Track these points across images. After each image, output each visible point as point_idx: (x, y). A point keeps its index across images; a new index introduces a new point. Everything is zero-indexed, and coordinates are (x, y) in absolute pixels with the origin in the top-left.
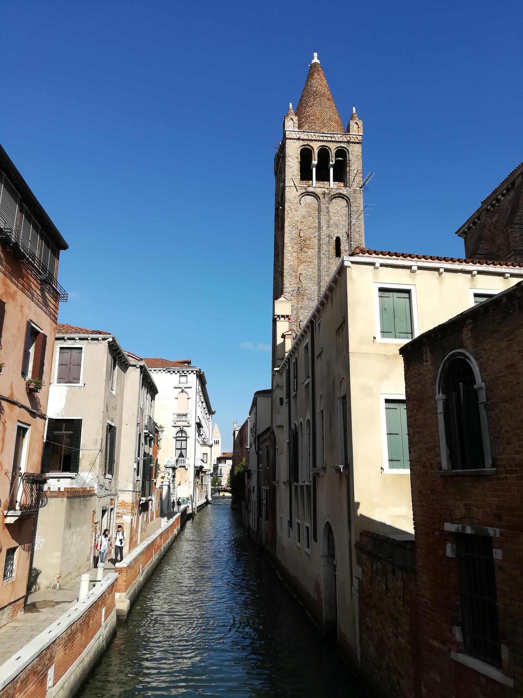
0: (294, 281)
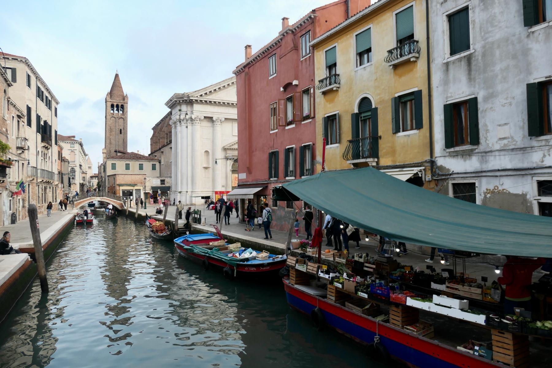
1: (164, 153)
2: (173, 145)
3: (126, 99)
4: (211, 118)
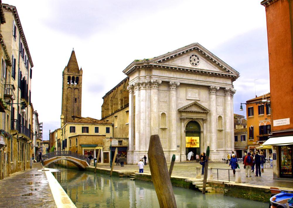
0: (66, 108)
1: (118, 118)
2: (130, 109)
3: (80, 72)
4: (167, 83)
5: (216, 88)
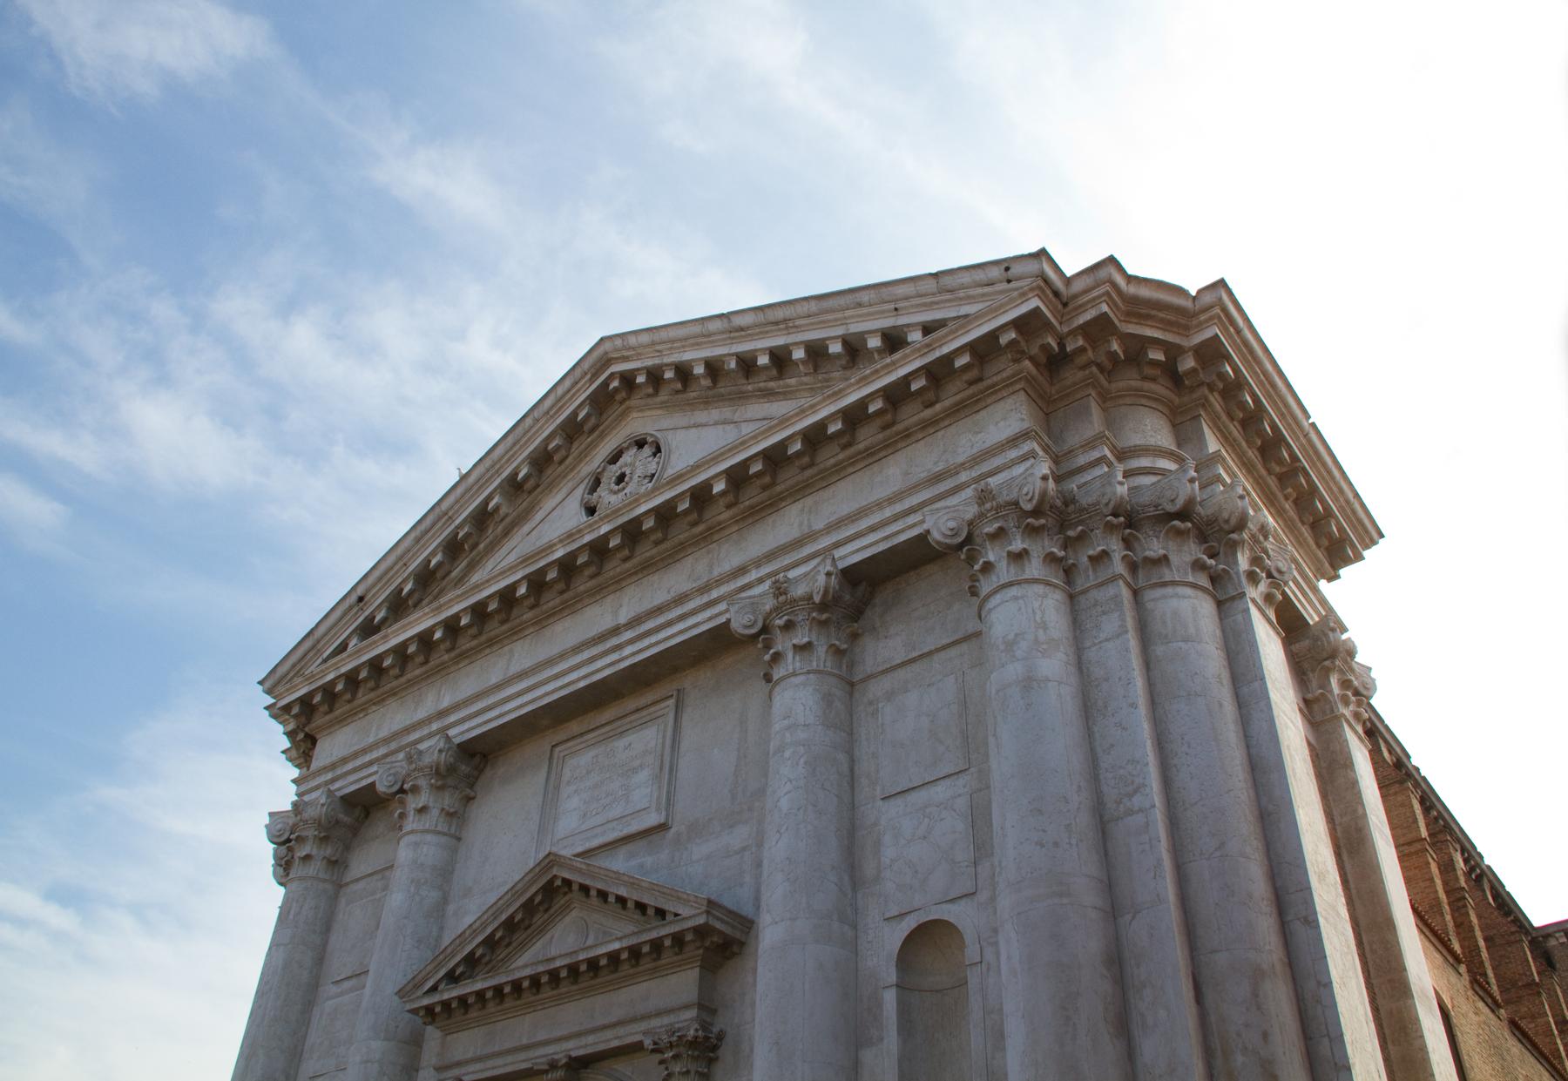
5: (799, 591)
